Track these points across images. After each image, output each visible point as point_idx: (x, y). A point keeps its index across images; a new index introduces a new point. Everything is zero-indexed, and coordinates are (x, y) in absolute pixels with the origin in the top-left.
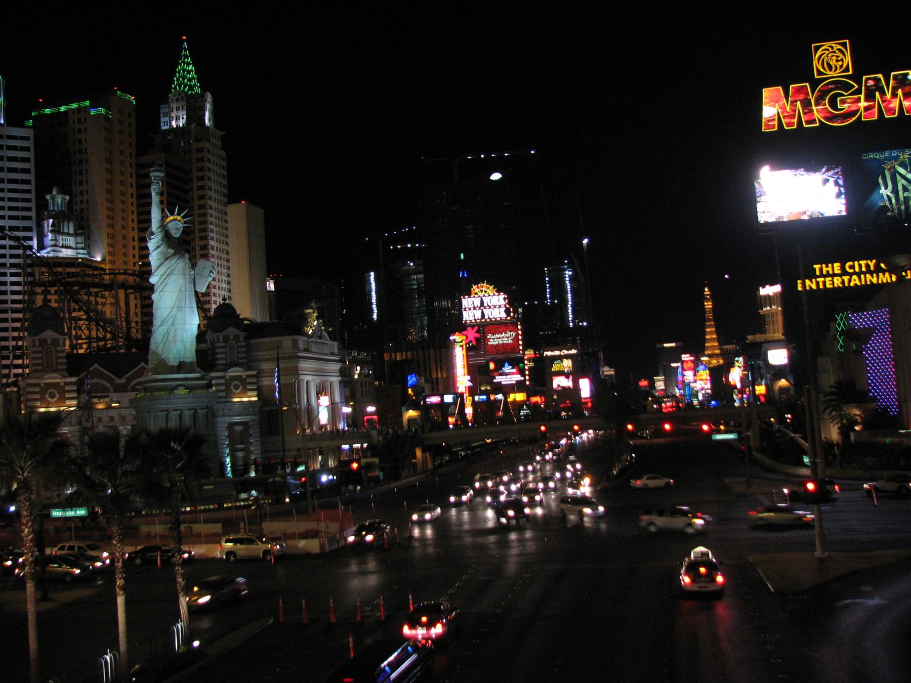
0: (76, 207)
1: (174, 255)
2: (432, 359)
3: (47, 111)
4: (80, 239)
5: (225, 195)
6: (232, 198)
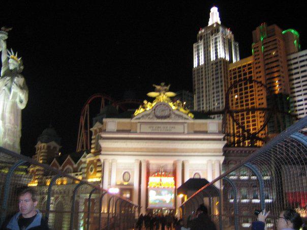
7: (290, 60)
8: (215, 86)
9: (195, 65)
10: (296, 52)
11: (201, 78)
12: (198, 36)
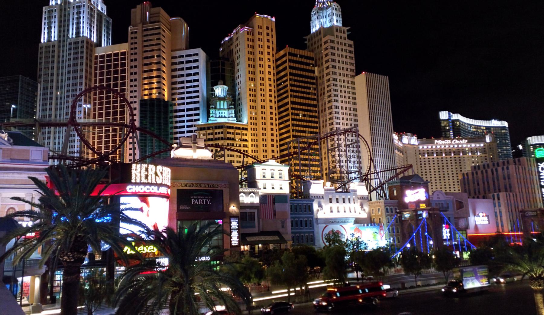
3: (226, 39)
5: (351, 70)
6: (358, 73)
7: (176, 57)
8: (71, 75)
9: (44, 38)
10: (183, 50)
11: (51, 59)
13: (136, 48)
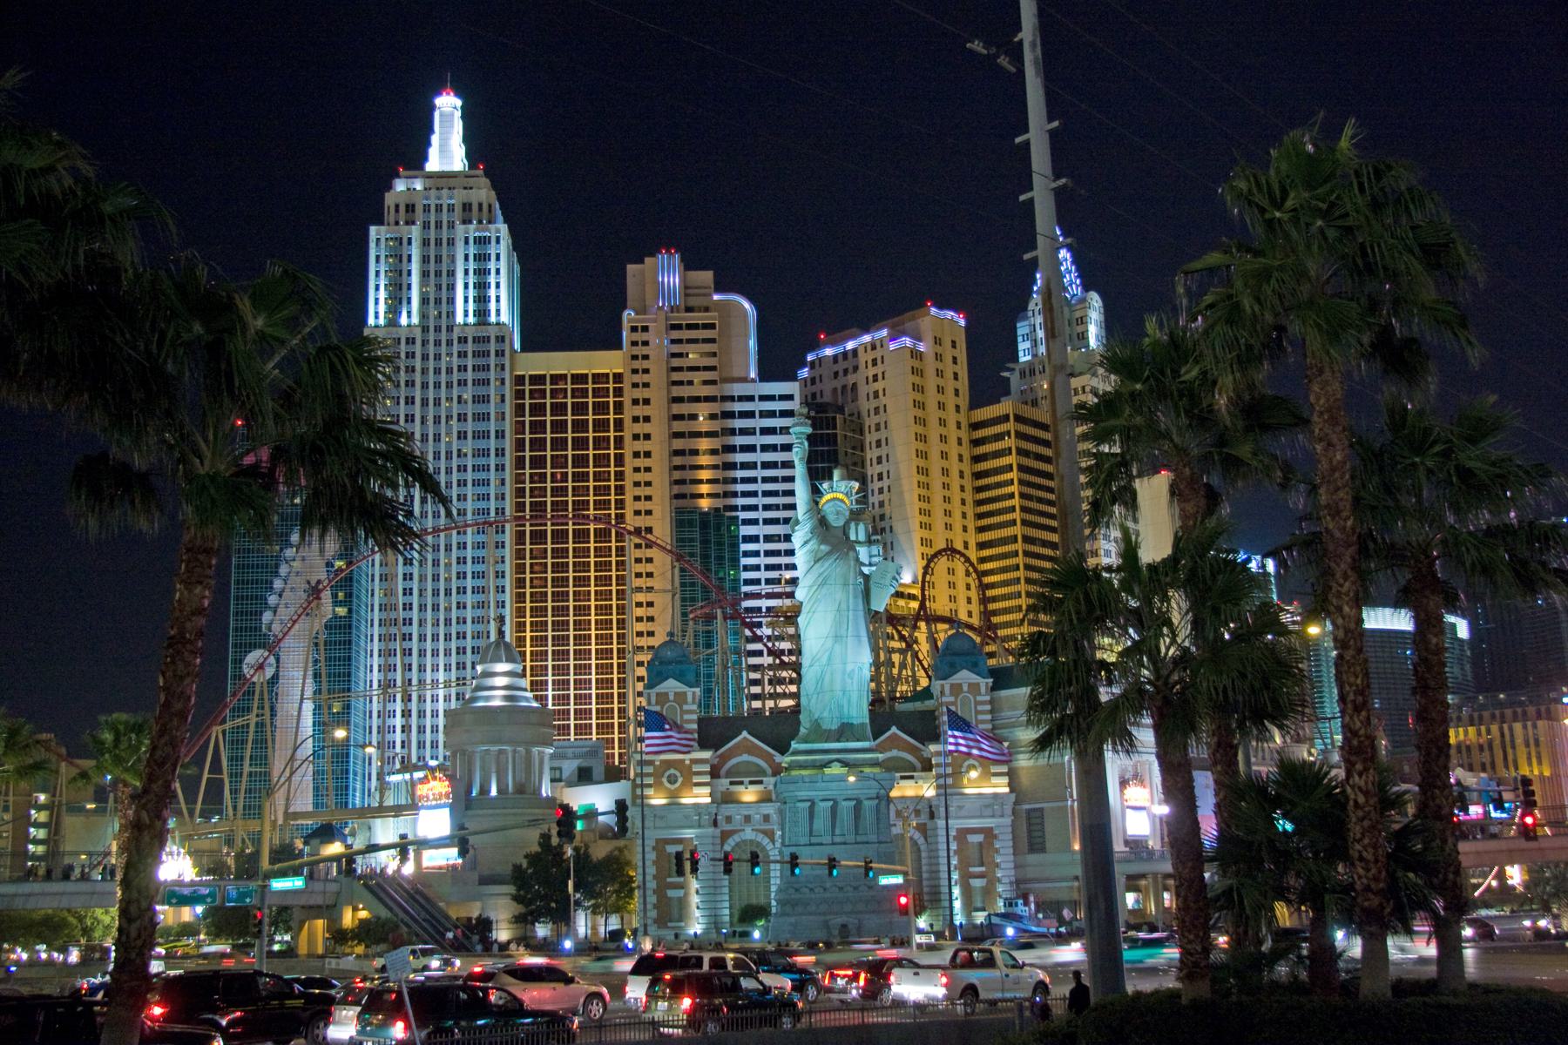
0: (874, 499)
1: (829, 554)
2: (1519, 741)
3: (829, 352)
4: (875, 549)
7: (732, 399)
12: (390, 199)
13: (646, 371)
